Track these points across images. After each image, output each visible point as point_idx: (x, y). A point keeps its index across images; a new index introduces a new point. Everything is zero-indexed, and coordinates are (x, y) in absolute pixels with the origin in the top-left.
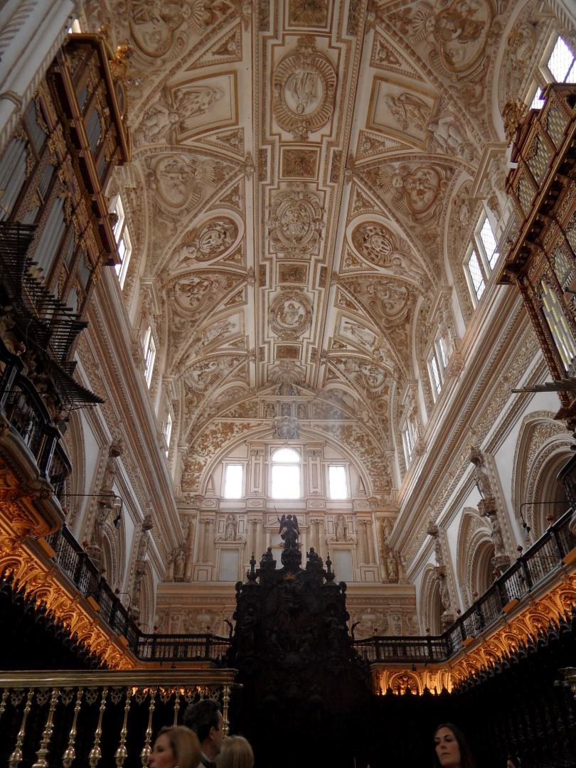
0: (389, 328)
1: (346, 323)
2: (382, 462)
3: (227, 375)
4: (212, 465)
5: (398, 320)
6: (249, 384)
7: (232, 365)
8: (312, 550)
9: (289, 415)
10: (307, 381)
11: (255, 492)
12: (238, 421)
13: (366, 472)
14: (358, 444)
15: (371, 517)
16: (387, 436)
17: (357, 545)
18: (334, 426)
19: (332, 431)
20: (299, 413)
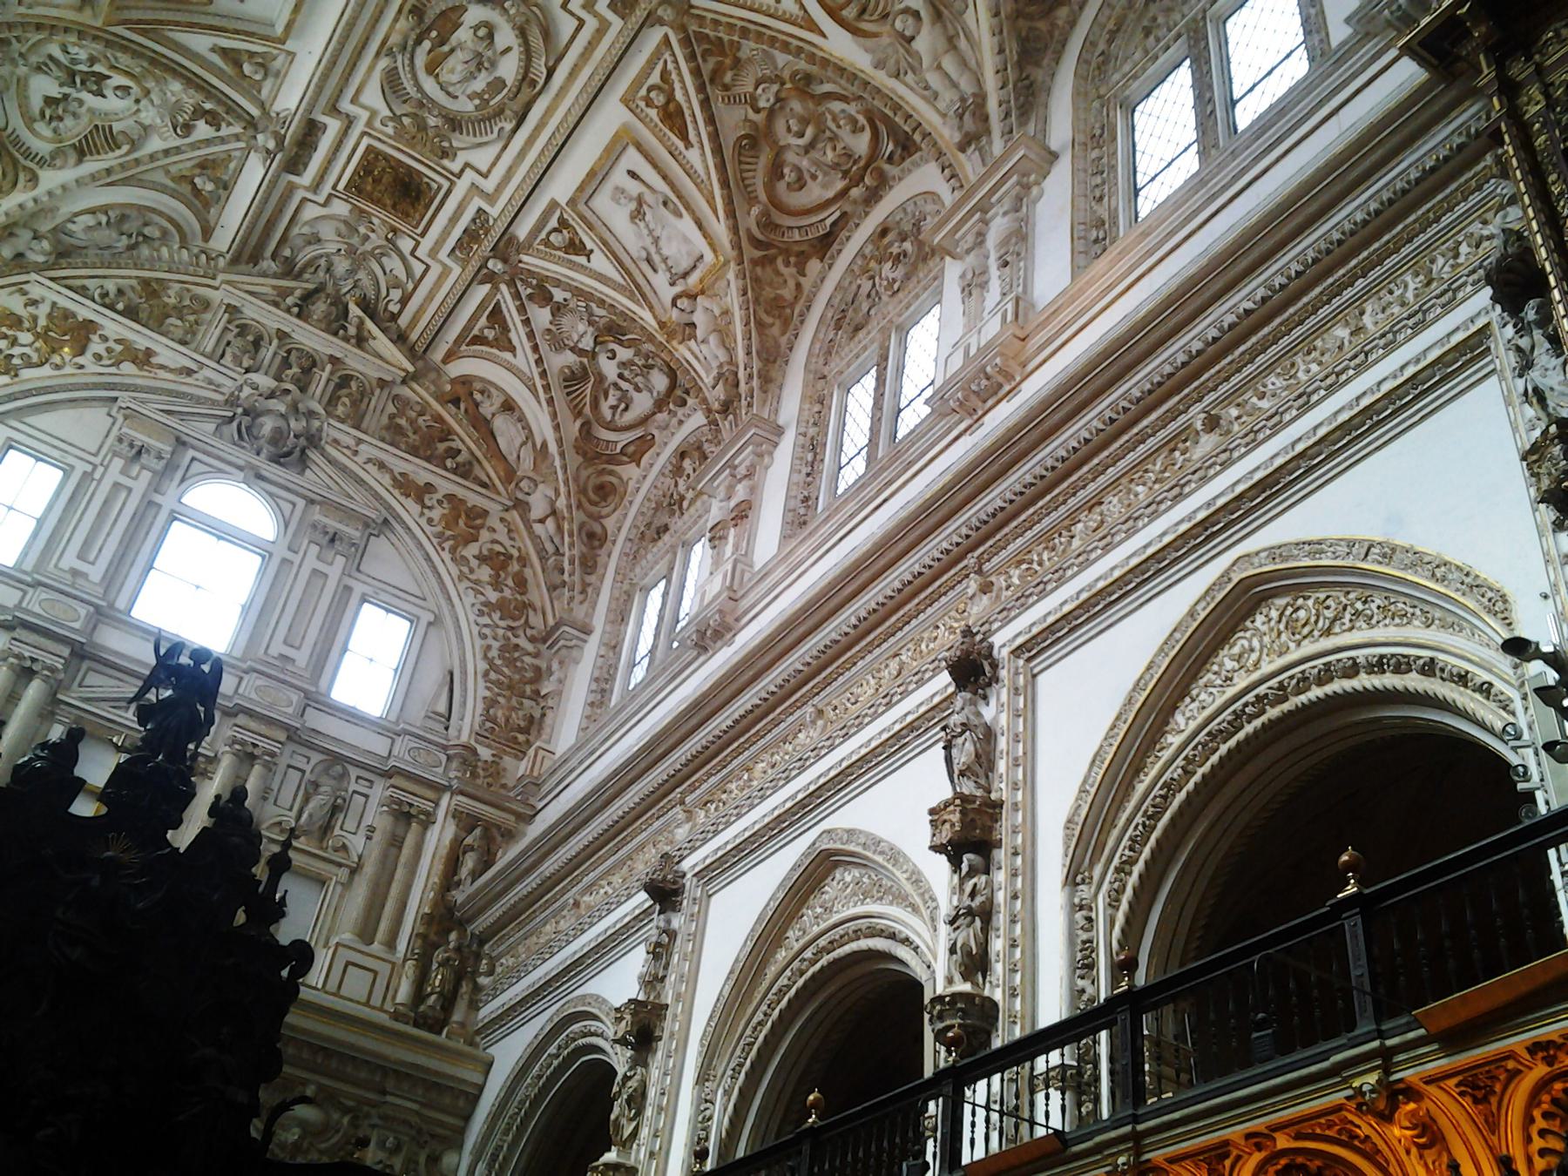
0: (757, 243)
1: (633, 174)
2: (537, 655)
3: (152, 157)
5: (796, 232)
6: (207, 233)
7: (188, 128)
8: (239, 794)
9: (303, 390)
10: (403, 321)
11: (75, 573)
12: (114, 327)
13: (475, 664)
14: (485, 573)
15: (437, 804)
17: (354, 871)
18: (429, 487)
19: (420, 500)
20: (332, 402)
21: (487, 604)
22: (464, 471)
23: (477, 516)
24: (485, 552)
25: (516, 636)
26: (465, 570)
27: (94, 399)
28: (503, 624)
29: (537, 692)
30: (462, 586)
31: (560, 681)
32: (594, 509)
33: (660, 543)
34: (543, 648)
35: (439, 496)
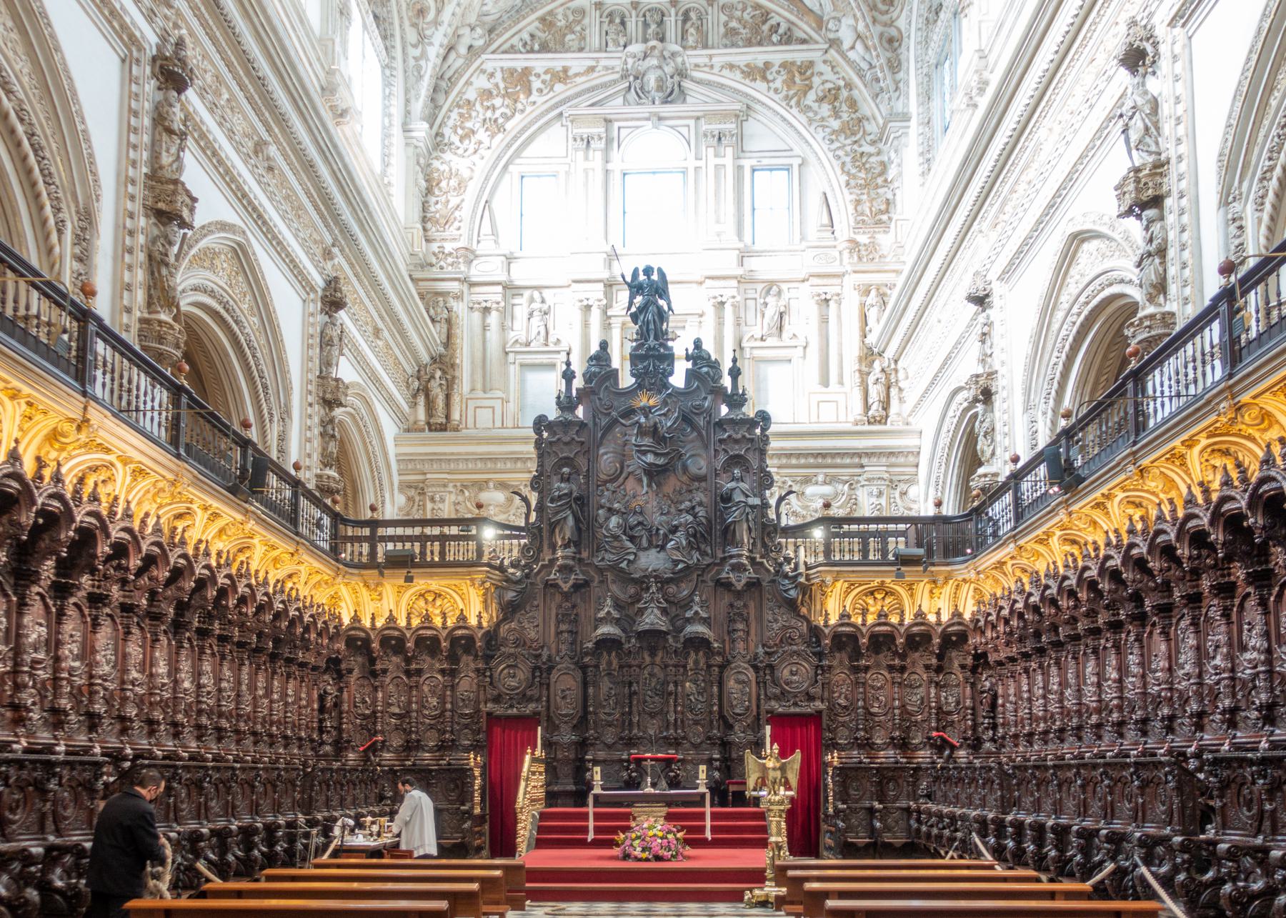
2: (879, 154)
4: (487, 179)
12: (540, 63)
14: (825, 109)
16: (897, 83)
18: (767, 65)
21: (834, 132)
22: (788, 39)
23: (806, 69)
24: (821, 94)
25: (860, 146)
26: (811, 114)
27: (551, 120)
28: (849, 141)
29: (886, 181)
30: (812, 129)
31: (899, 165)
32: (885, 18)
33: (939, 23)
34: (881, 145)
35: (776, 68)
